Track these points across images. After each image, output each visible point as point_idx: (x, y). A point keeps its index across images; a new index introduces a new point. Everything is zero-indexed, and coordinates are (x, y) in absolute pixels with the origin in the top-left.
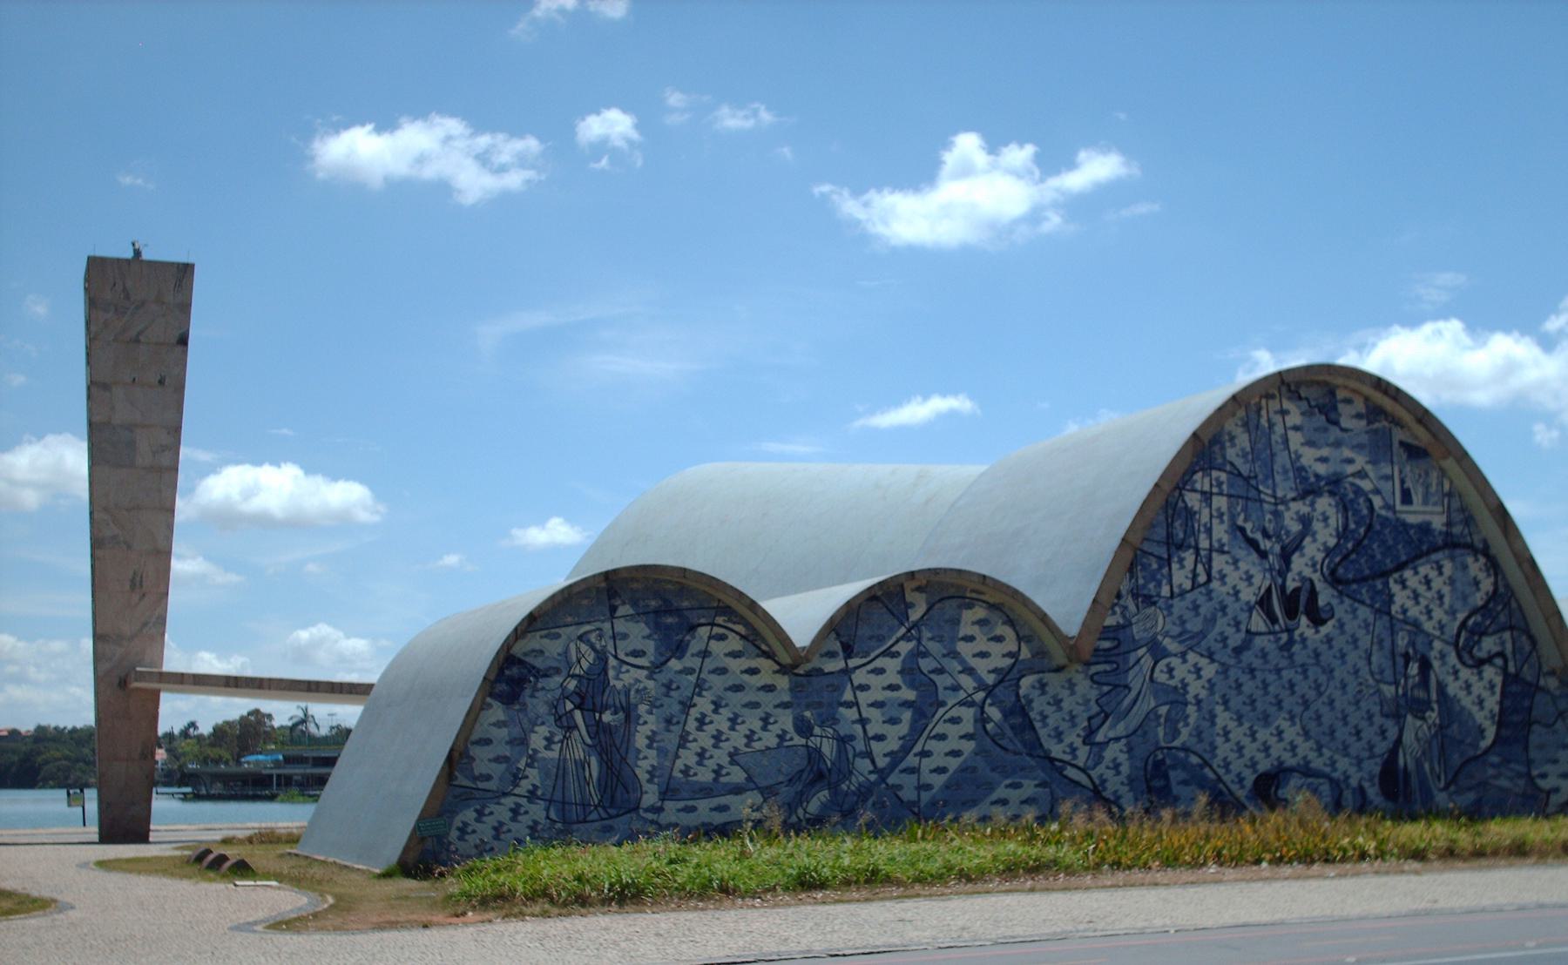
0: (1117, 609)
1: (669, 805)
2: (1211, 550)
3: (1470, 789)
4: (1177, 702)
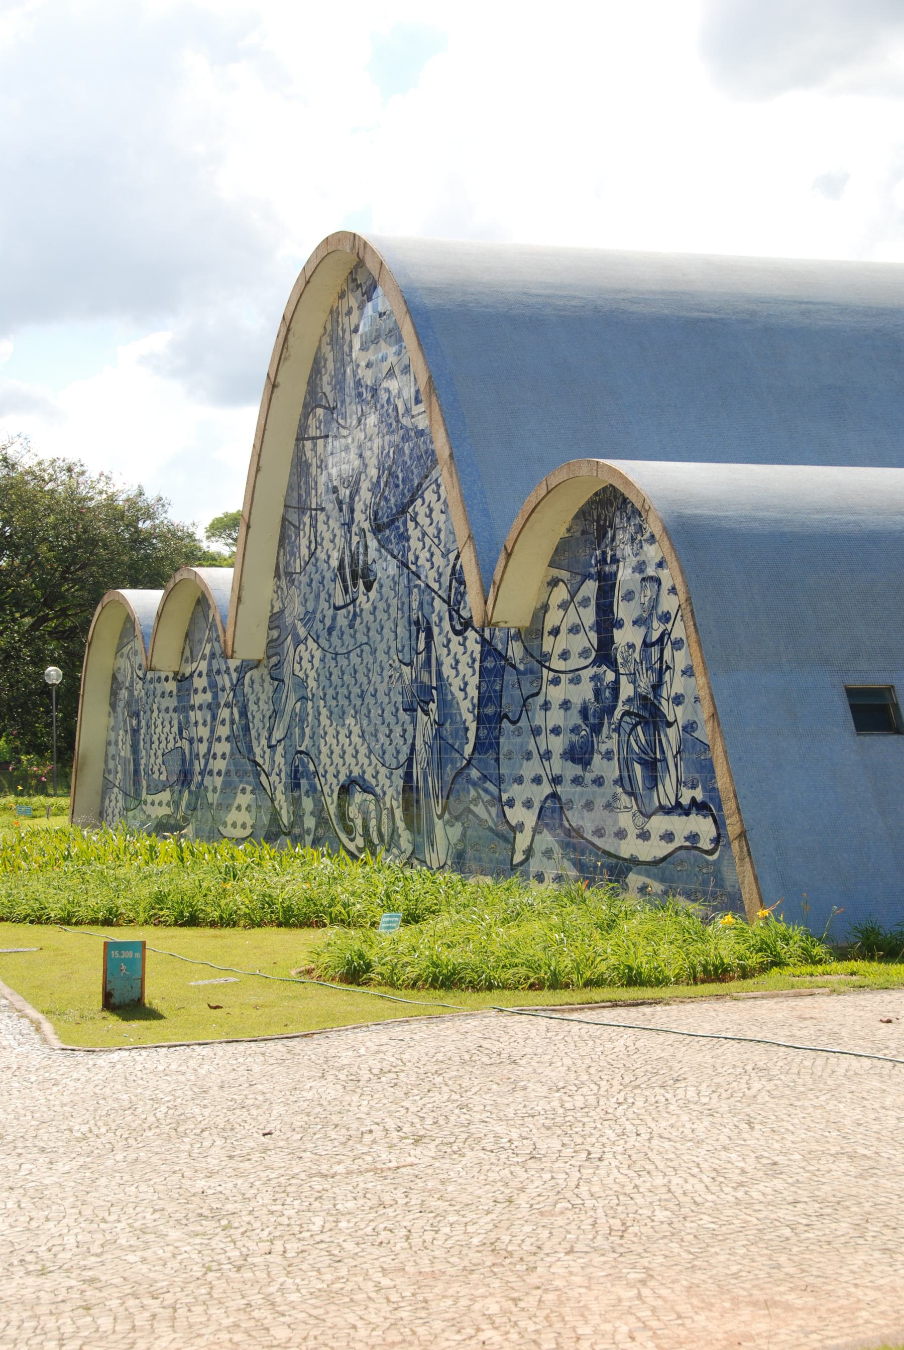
0: (279, 592)
1: (150, 798)
2: (315, 510)
3: (457, 818)
4: (303, 697)
